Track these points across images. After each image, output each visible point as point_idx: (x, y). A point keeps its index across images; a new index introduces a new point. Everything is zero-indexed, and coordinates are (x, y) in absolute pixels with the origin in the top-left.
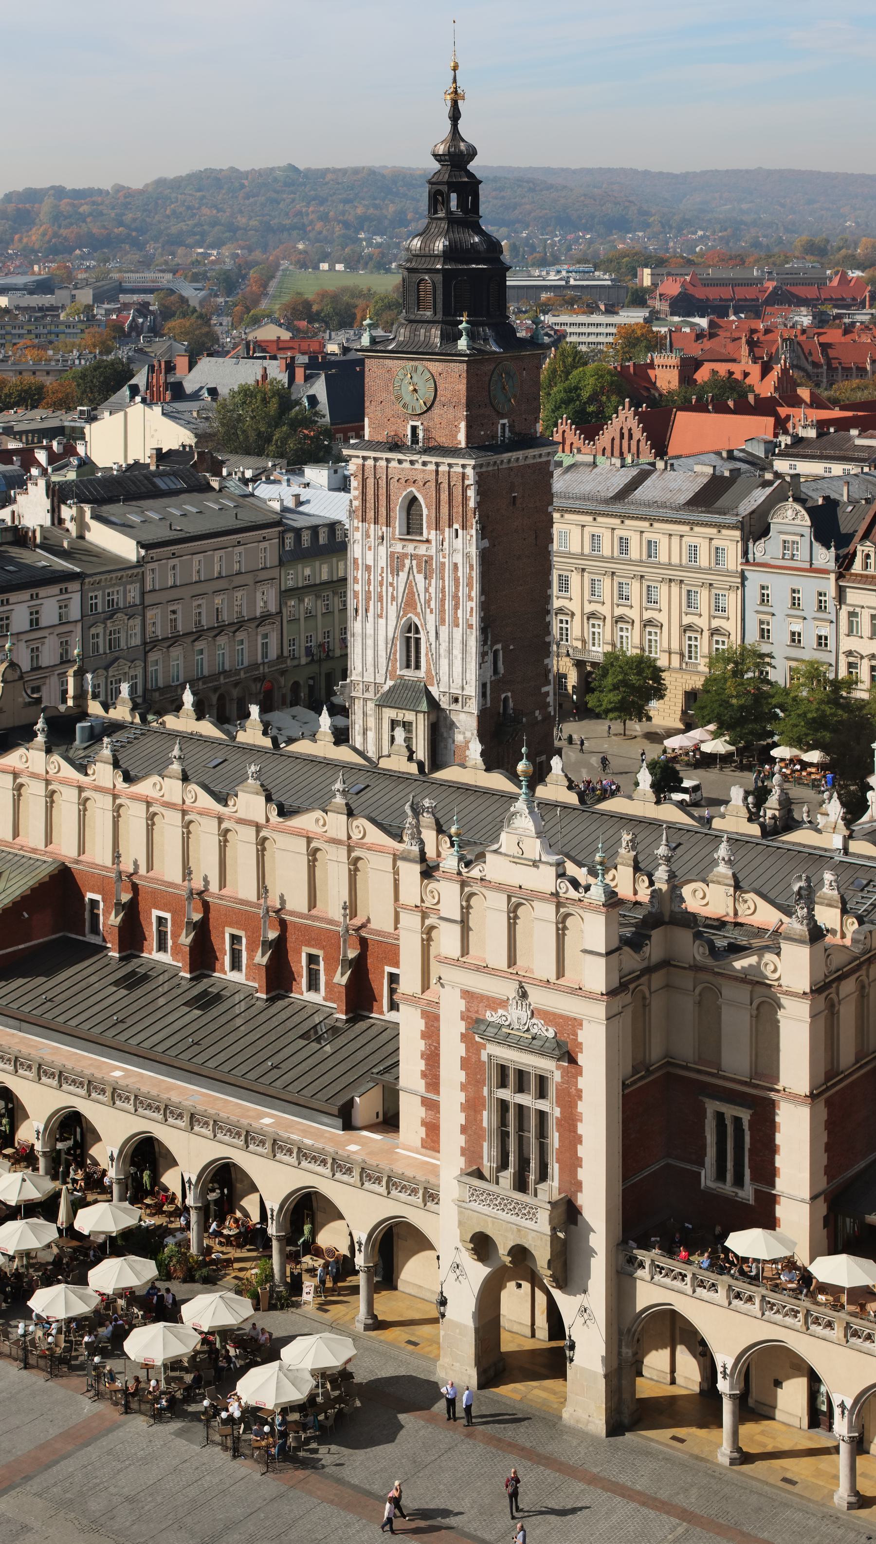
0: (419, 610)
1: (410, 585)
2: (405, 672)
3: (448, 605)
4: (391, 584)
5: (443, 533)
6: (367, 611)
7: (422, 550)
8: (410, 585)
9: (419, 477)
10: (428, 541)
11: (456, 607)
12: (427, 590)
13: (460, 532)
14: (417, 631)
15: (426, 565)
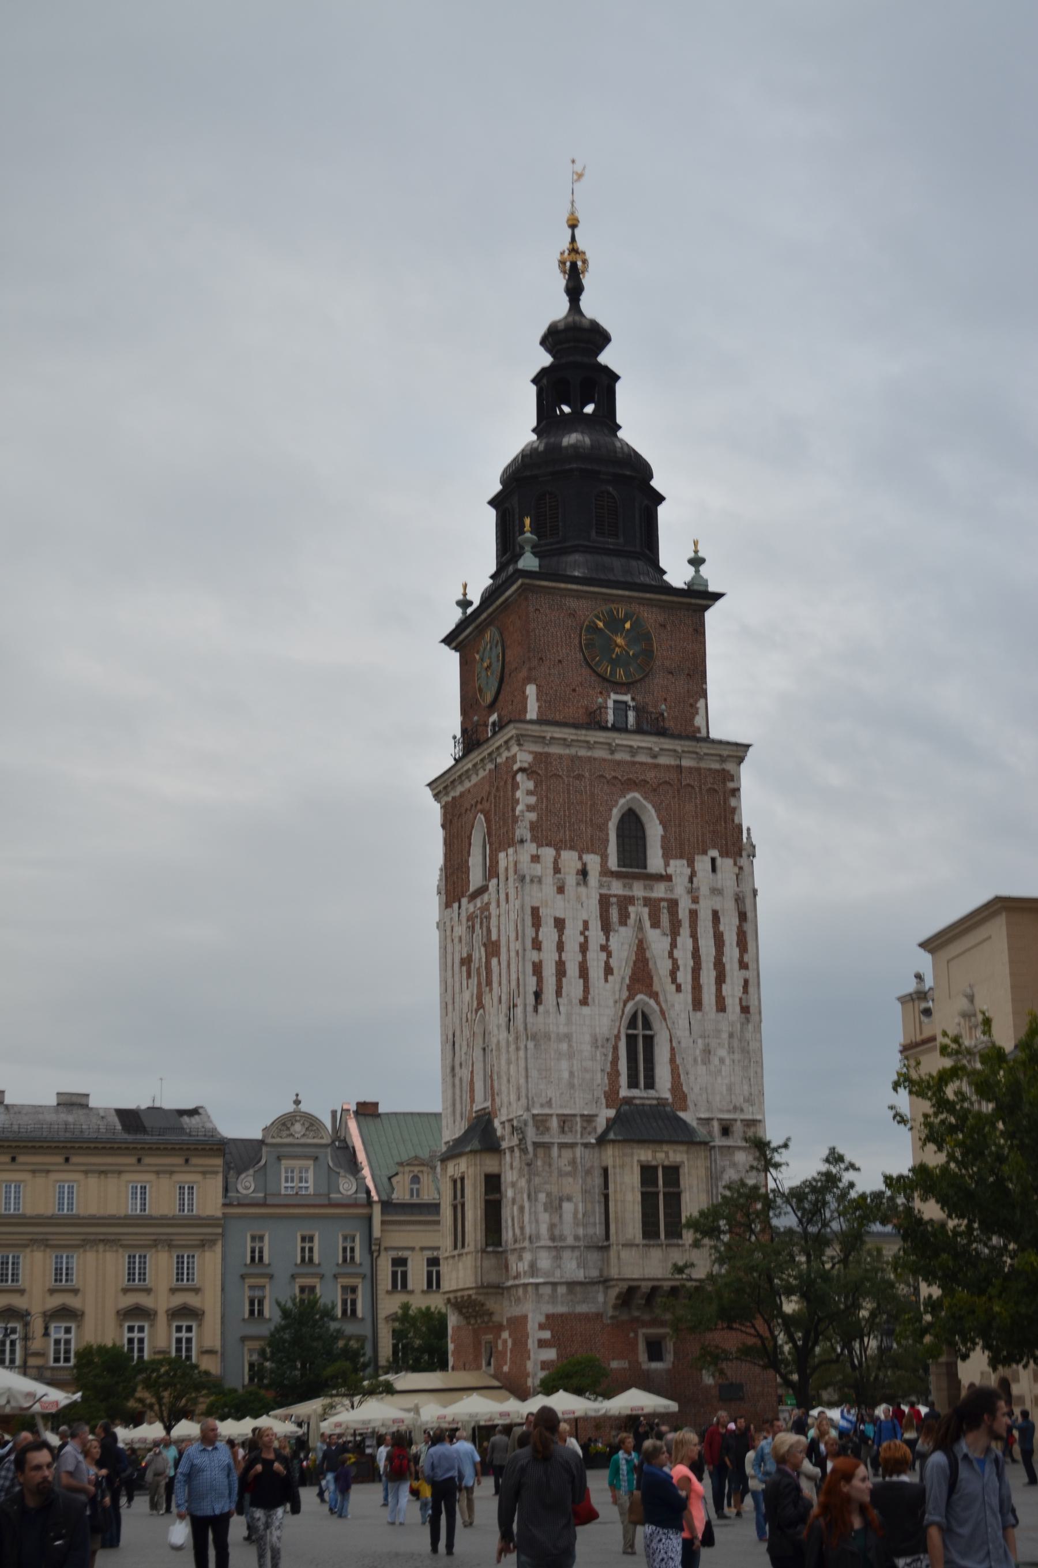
0: (656, 987)
1: (641, 948)
2: (635, 1092)
3: (708, 976)
4: (604, 948)
5: (691, 863)
6: (559, 993)
7: (659, 891)
8: (641, 948)
9: (650, 775)
10: (668, 878)
11: (720, 979)
12: (671, 955)
13: (719, 861)
14: (647, 1024)
15: (665, 914)
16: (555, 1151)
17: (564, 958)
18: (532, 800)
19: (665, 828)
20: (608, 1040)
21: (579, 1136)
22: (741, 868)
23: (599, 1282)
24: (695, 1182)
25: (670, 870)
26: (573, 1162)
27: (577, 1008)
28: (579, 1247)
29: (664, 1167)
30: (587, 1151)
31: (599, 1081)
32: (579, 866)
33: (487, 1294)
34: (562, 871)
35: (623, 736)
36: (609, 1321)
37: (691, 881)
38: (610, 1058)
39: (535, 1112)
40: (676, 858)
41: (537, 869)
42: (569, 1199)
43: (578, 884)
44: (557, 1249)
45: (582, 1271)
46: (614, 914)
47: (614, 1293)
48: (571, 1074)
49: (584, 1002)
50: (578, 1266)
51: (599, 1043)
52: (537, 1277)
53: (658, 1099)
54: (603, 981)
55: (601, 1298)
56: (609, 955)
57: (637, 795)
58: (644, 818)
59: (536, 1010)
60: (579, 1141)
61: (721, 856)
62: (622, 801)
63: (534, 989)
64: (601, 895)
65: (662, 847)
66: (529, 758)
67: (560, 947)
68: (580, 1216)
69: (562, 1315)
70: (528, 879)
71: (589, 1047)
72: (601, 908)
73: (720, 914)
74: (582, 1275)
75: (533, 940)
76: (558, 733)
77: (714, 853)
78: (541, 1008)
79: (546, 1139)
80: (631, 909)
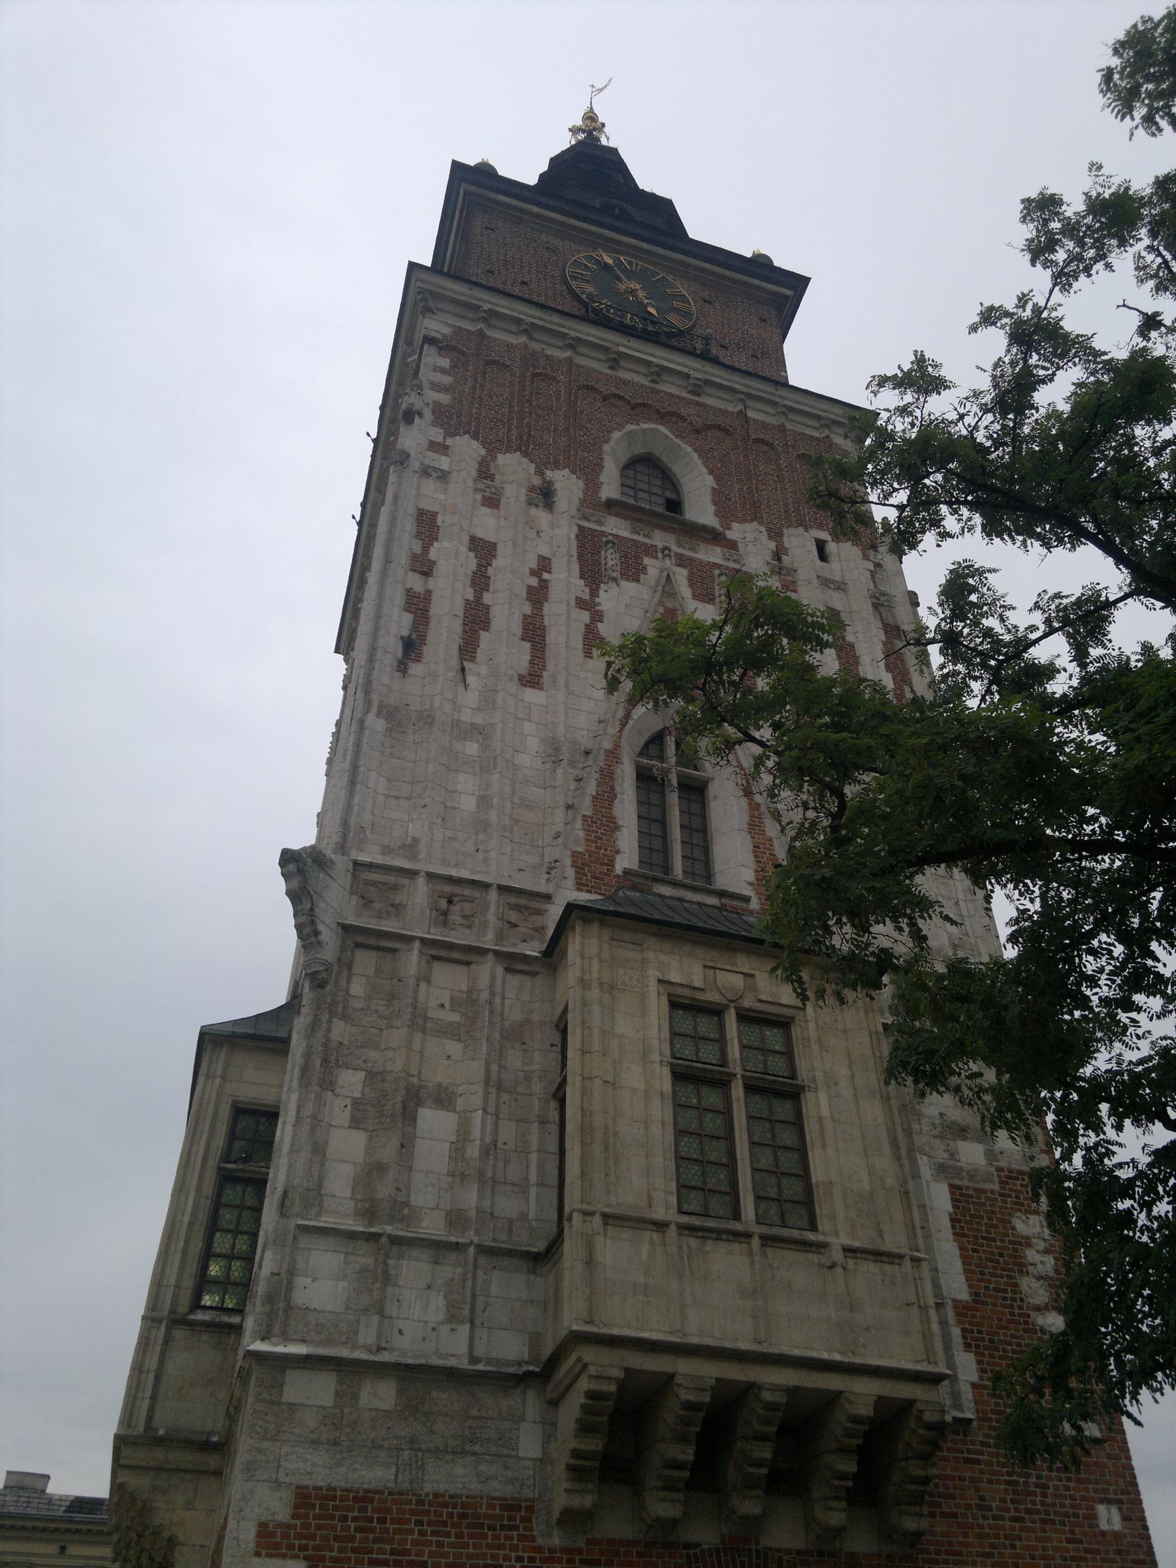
6: (468, 650)
13: (832, 547)
16: (412, 959)
17: (487, 598)
18: (447, 380)
19: (718, 479)
20: (587, 753)
21: (490, 935)
22: (878, 565)
23: (522, 1380)
24: (843, 1071)
25: (730, 535)
26: (467, 1002)
27: (513, 687)
28: (457, 1247)
29: (746, 1017)
30: (514, 981)
31: (560, 827)
32: (537, 481)
33: (160, 1469)
34: (498, 477)
35: (634, 343)
36: (557, 1540)
37: (779, 559)
38: (592, 788)
39: (363, 858)
40: (745, 521)
41: (444, 463)
42: (444, 1099)
43: (530, 503)
44: (381, 1237)
45: (465, 1329)
46: (611, 558)
47: (571, 1410)
48: (483, 801)
49: (532, 679)
50: (451, 1318)
51: (565, 754)
52: (286, 1338)
53: (722, 894)
54: (581, 654)
55: (529, 1444)
56: (597, 616)
57: (662, 428)
58: (677, 470)
59: (402, 668)
60: (488, 940)
61: (836, 539)
62: (630, 427)
63: (405, 633)
64: (580, 528)
65: (715, 503)
66: (447, 331)
67: (480, 581)
68: (473, 1151)
69: (363, 1498)
70: (415, 465)
71: (540, 766)
72: (581, 546)
73: (843, 616)
74: (463, 1349)
75: (414, 557)
76: (505, 306)
77: (824, 535)
78: (416, 669)
79: (389, 925)
80: (646, 561)
